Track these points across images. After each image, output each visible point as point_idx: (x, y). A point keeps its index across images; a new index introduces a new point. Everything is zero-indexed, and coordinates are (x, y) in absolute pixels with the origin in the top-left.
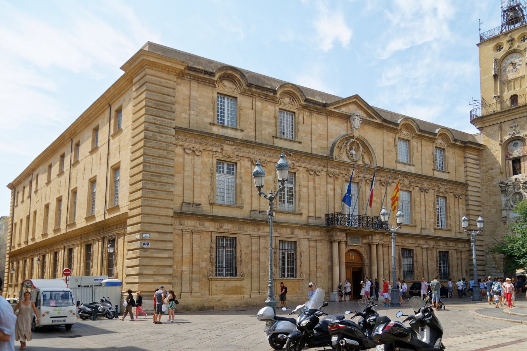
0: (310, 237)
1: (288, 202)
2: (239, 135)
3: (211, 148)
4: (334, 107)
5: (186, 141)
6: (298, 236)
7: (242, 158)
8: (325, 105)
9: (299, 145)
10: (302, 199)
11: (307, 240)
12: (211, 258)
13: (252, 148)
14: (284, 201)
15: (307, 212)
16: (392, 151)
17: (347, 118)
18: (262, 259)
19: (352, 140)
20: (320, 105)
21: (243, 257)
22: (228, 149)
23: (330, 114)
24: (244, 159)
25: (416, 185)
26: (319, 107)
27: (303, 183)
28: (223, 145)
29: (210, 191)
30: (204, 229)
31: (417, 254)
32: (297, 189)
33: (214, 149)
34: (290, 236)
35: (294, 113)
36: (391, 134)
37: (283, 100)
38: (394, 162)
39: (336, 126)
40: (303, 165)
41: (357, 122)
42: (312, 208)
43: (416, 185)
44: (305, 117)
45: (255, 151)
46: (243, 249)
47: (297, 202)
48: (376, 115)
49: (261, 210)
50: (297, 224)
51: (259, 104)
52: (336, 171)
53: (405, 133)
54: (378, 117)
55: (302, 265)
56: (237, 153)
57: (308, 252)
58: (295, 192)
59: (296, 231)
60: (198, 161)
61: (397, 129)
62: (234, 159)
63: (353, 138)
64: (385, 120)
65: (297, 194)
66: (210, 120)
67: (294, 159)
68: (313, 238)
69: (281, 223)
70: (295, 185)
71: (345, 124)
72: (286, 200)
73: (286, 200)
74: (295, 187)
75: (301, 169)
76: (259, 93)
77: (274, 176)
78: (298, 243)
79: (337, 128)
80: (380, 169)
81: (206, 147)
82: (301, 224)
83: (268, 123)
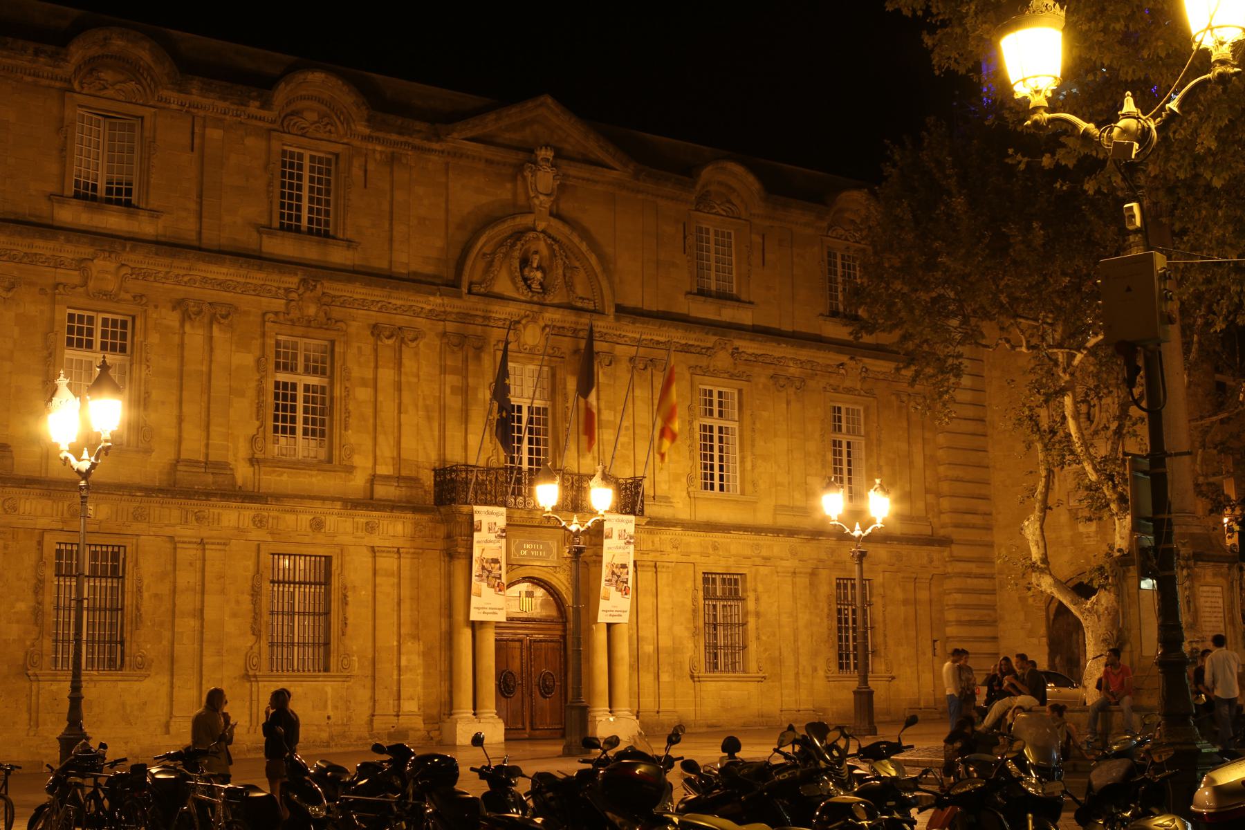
1: (305, 432)
12: (38, 612)
14: (293, 431)
15: (370, 465)
18: (209, 614)
21: (147, 604)
31: (760, 588)
32: (337, 392)
34: (307, 540)
37: (296, 119)
42: (386, 449)
44: (371, 166)
46: (146, 582)
47: (336, 431)
49: (212, 458)
55: (350, 628)
57: (370, 587)
58: (332, 399)
65: (337, 407)
66: (52, 188)
70: (332, 378)
72: (300, 426)
73: (300, 426)
74: (332, 384)
77: (258, 353)
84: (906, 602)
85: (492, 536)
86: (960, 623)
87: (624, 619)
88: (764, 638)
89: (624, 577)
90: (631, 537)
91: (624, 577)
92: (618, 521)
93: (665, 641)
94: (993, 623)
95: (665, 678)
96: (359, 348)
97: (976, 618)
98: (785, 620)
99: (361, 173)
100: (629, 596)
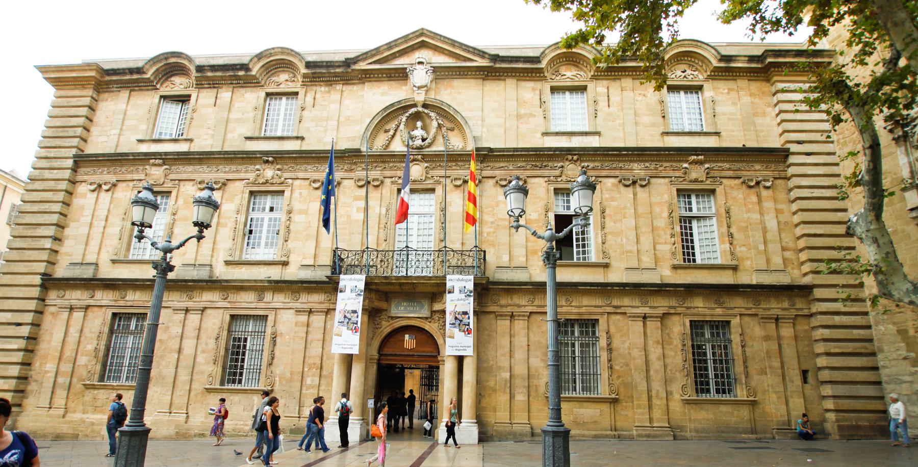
0: (298, 305)
2: (183, 147)
3: (129, 177)
4: (370, 61)
5: (95, 173)
6: (271, 305)
7: (182, 183)
8: (348, 63)
9: (299, 142)
10: (292, 236)
11: (293, 311)
13: (201, 164)
16: (531, 115)
17: (401, 75)
19: (413, 110)
20: (339, 66)
22: (156, 173)
23: (367, 76)
24: (187, 183)
25: (604, 173)
26: (338, 70)
27: (296, 206)
28: (147, 167)
29: (117, 241)
30: (92, 302)
33: (136, 177)
34: (252, 306)
35: (296, 94)
36: (531, 84)
38: (539, 135)
39: (383, 94)
40: (301, 175)
41: (420, 76)
43: (604, 173)
45: (205, 167)
48: (474, 53)
50: (261, 281)
51: (225, 94)
52: (375, 174)
53: (569, 75)
54: (479, 55)
56: (172, 176)
59: (268, 296)
60: (105, 197)
61: (540, 71)
62: (168, 186)
63: (415, 105)
64: (495, 58)
67: (278, 167)
68: (305, 306)
69: (227, 281)
71: (404, 88)
75: (297, 182)
76: (222, 78)
78: (269, 318)
79: (380, 96)
80: (486, 156)
81: (121, 177)
82: (270, 282)
83: (239, 121)
84: (767, 338)
85: (354, 295)
86: (828, 354)
87: (469, 352)
88: (617, 368)
89: (465, 321)
90: (471, 292)
91: (465, 321)
92: (459, 280)
93: (520, 369)
94: (873, 354)
95: (521, 397)
96: (301, 194)
97: (850, 350)
98: (638, 354)
99: (312, 100)
100: (472, 335)
